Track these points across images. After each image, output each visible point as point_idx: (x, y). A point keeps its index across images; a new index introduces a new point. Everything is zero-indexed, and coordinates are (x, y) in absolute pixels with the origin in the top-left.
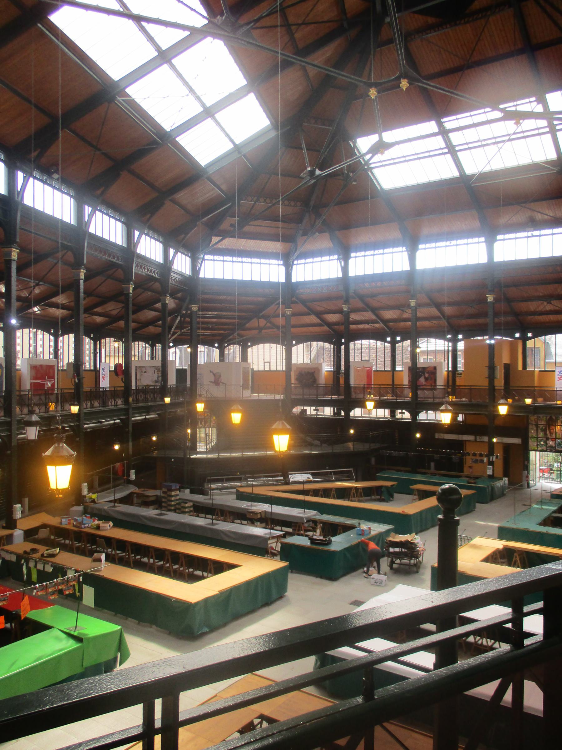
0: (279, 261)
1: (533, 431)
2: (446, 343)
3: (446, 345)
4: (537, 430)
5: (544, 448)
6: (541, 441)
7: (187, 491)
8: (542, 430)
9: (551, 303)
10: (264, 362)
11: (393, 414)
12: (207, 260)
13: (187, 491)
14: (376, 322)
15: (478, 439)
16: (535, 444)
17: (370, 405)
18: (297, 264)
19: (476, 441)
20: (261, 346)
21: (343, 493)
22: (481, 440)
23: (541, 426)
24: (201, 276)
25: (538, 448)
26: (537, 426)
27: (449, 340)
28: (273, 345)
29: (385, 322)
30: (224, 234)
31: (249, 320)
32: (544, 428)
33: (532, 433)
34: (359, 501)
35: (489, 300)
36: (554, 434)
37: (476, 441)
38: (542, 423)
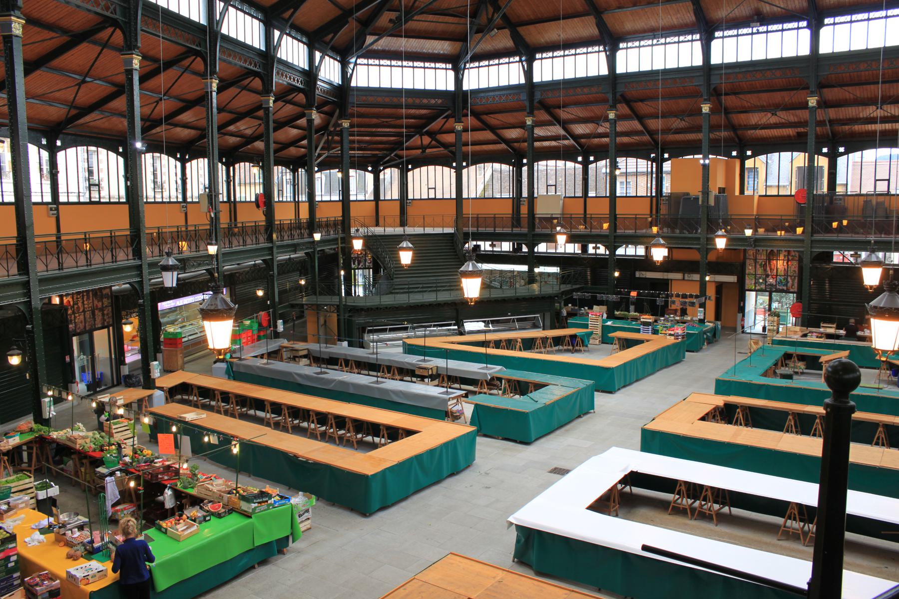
0: (447, 65)
1: (750, 268)
3: (649, 166)
4: (755, 266)
5: (763, 286)
6: (760, 278)
7: (345, 344)
8: (761, 265)
9: (776, 115)
10: (428, 189)
11: (584, 249)
12: (360, 64)
13: (345, 344)
14: (565, 138)
15: (686, 277)
17: (561, 239)
19: (684, 279)
20: (424, 169)
21: (529, 344)
22: (690, 279)
23: (761, 261)
24: (353, 84)
26: (755, 260)
27: (653, 160)
28: (439, 168)
29: (576, 137)
30: (380, 33)
31: (409, 137)
32: (763, 263)
33: (750, 269)
34: (548, 353)
36: (775, 270)
37: (684, 279)
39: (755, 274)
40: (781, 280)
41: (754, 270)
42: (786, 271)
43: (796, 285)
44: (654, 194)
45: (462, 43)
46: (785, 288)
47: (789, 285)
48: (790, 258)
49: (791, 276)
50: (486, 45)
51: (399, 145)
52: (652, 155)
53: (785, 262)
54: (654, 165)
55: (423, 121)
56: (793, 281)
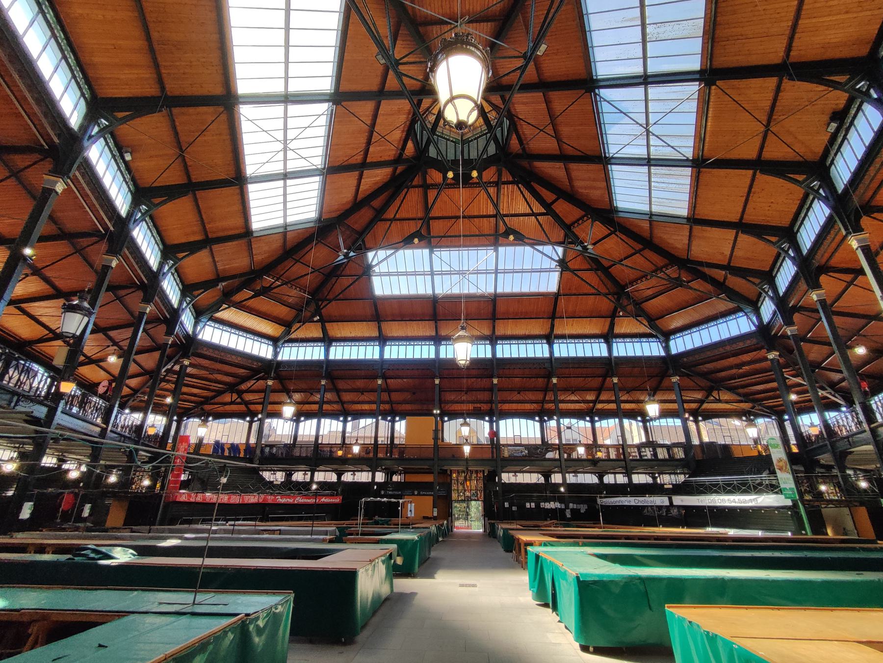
2: (387, 423)
5: (463, 498)
8: (461, 483)
12: (208, 325)
18: (284, 347)
24: (200, 337)
26: (457, 480)
27: (389, 421)
33: (454, 487)
35: (436, 383)
38: (461, 478)
39: (458, 490)
43: (483, 496)
44: (389, 443)
46: (476, 498)
47: (479, 496)
51: (207, 400)
52: (389, 418)
54: (390, 423)
55: (238, 380)
56: (481, 494)
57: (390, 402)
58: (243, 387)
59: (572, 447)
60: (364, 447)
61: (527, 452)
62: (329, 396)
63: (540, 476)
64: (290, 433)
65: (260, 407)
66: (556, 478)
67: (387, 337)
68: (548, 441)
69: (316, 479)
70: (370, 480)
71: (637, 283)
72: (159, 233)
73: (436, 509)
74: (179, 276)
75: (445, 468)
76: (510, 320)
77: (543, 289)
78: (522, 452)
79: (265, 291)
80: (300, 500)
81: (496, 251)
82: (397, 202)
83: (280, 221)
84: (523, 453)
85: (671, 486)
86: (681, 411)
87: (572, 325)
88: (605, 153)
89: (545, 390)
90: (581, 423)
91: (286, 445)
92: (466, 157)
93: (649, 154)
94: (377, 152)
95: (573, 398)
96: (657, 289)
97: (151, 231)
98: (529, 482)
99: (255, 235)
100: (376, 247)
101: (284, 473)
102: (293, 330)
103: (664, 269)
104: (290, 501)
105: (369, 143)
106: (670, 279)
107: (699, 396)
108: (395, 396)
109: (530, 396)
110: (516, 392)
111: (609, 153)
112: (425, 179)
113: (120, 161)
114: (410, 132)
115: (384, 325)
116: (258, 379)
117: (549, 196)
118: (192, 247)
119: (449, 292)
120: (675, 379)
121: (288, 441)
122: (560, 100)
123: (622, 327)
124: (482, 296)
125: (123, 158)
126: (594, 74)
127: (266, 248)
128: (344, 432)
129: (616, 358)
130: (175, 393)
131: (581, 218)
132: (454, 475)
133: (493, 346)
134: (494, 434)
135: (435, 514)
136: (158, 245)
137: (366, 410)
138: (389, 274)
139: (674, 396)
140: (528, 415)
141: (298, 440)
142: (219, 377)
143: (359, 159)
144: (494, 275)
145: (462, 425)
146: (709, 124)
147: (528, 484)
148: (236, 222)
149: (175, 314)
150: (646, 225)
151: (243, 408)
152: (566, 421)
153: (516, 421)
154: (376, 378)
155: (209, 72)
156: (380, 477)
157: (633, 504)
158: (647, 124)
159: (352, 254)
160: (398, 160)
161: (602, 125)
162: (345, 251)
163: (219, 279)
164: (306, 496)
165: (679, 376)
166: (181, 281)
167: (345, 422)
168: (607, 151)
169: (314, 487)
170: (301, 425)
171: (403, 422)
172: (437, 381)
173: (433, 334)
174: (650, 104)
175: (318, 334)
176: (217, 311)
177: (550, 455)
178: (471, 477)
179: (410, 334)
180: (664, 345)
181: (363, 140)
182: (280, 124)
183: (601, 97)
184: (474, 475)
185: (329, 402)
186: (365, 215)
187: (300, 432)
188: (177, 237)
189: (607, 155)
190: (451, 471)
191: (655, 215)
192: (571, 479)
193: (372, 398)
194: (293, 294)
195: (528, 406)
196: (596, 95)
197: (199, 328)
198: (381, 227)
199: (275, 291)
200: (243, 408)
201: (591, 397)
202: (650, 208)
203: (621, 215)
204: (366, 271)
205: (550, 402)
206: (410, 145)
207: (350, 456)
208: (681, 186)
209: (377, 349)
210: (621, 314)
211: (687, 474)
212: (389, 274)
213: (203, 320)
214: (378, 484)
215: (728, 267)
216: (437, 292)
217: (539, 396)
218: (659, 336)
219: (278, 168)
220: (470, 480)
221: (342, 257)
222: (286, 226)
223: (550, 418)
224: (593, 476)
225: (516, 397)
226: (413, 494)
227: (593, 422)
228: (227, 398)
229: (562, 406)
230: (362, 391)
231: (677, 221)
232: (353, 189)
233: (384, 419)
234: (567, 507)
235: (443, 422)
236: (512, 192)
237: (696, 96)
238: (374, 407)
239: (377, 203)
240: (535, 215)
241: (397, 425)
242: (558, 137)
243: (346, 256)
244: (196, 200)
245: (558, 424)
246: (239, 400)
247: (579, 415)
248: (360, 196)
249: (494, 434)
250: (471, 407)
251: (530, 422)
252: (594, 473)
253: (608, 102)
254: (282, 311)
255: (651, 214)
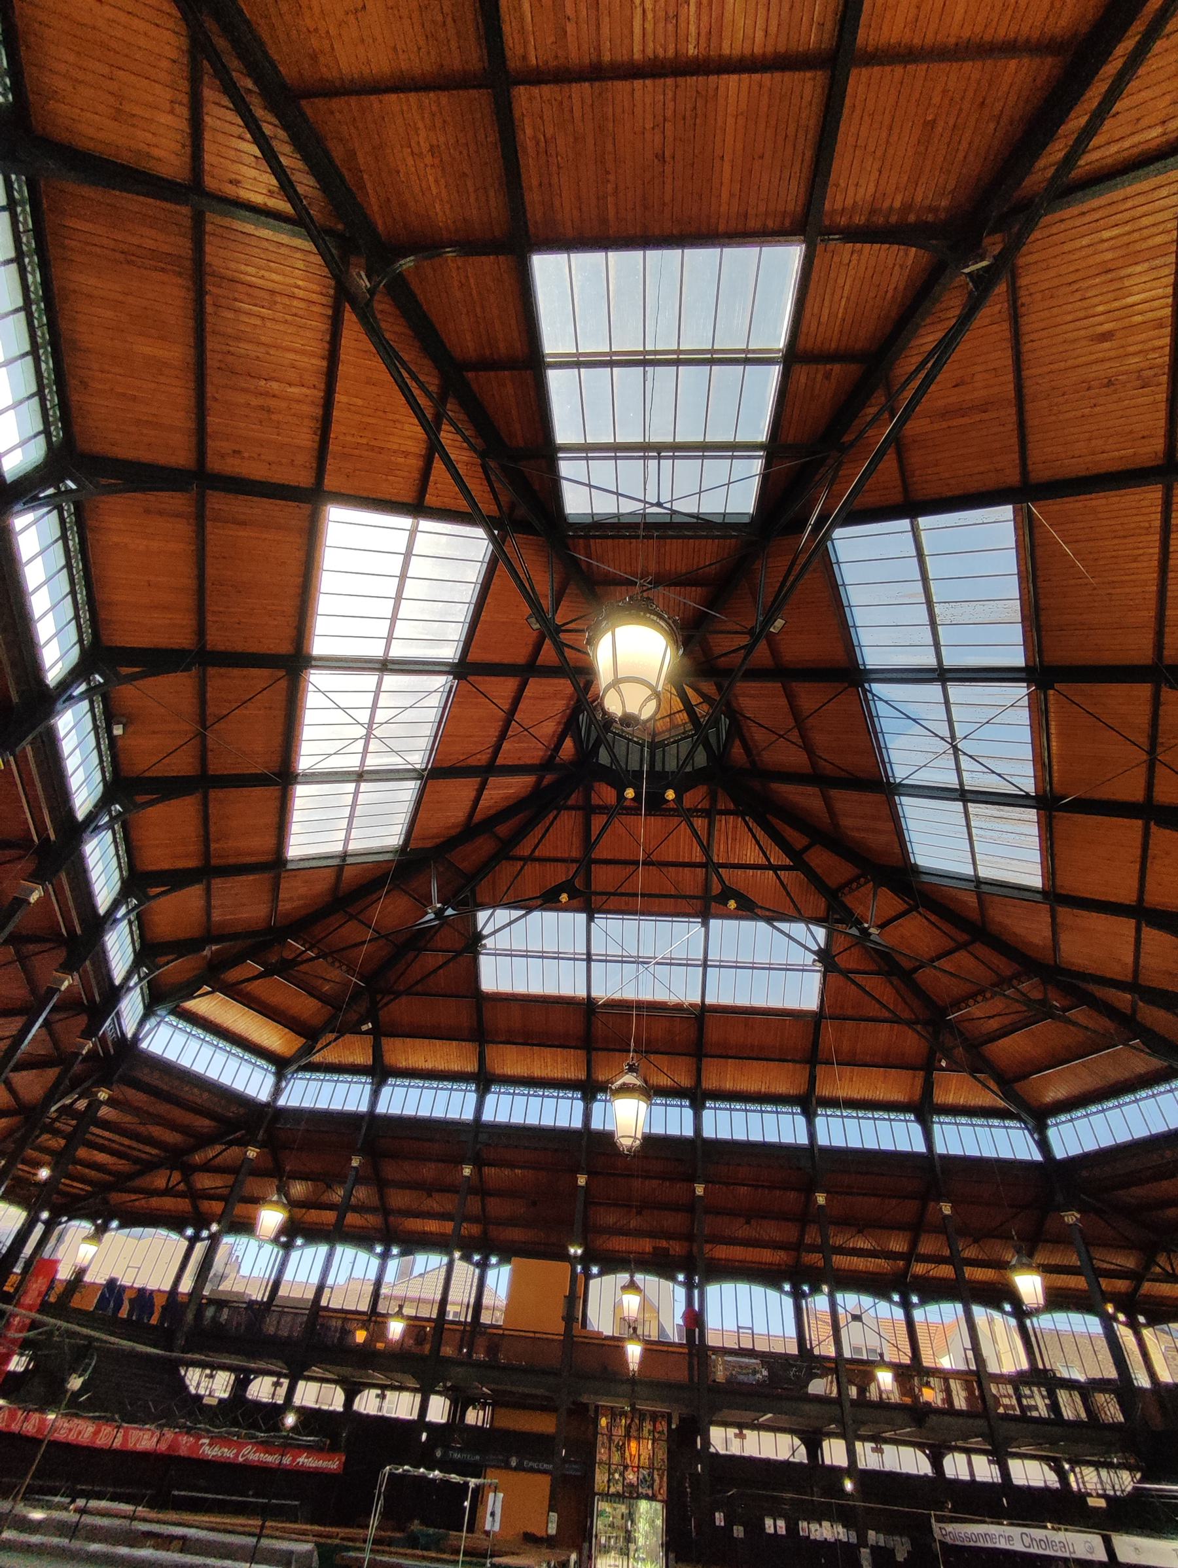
2: (471, 1268)
5: (620, 1488)
6: (616, 1471)
16: (606, 1479)
18: (296, 1078)
24: (144, 1045)
25: (609, 1487)
27: (477, 1265)
33: (602, 1454)
39: (610, 1465)
40: (644, 1478)
41: (607, 1456)
42: (651, 1459)
43: (665, 1485)
44: (469, 1320)
45: (303, 1040)
47: (656, 1486)
48: (657, 1435)
49: (658, 1470)
50: (329, 1055)
51: (120, 1182)
53: (650, 1442)
57: (482, 1219)
58: (198, 1158)
59: (861, 1371)
60: (415, 1326)
61: (765, 1373)
62: (362, 1194)
63: (797, 1442)
64: (267, 1276)
65: (217, 1207)
66: (834, 1452)
67: (494, 1075)
68: (812, 1348)
69: (297, 1401)
70: (415, 1416)
71: (968, 1006)
72: (129, 851)
73: (554, 1516)
74: (140, 927)
75: (585, 1399)
76: (730, 1060)
77: (792, 1003)
78: (755, 1372)
79: (285, 968)
80: (251, 1454)
81: (705, 924)
82: (539, 831)
83: (338, 848)
84: (758, 1376)
85: (1102, 1503)
86: (1098, 1297)
87: (851, 1080)
88: (887, 777)
89: (805, 1216)
90: (883, 1307)
91: (252, 1303)
92: (658, 768)
93: (961, 783)
94: (511, 752)
95: (862, 1243)
96: (1007, 1020)
97: (116, 847)
98: (772, 1456)
99: (290, 866)
100: (495, 904)
101: (233, 1377)
102: (319, 1046)
103: (1015, 982)
104: (228, 1453)
105: (503, 736)
106: (1028, 1001)
107: (1128, 1262)
108: (496, 1206)
109: (771, 1230)
110: (742, 1220)
111: (893, 776)
112: (588, 798)
113: (102, 732)
114: (570, 725)
115: (492, 1051)
116: (230, 1144)
117: (798, 840)
118: (176, 879)
119: (617, 996)
120: (1071, 1217)
121: (258, 1294)
122: (809, 696)
123: (947, 1091)
124: (678, 1008)
125: (109, 730)
126: (860, 662)
127: (303, 890)
128: (378, 1283)
129: (943, 1157)
130: (59, 1160)
131: (856, 879)
132: (603, 1422)
133: (698, 1109)
134: (695, 1320)
135: (552, 1530)
136: (121, 871)
137: (431, 1233)
138: (511, 954)
139: (1075, 1257)
140: (769, 1277)
141: (280, 1293)
142: (157, 1131)
143: (483, 759)
144: (701, 969)
145: (625, 1288)
146: (1054, 744)
147: (767, 1462)
148: (261, 844)
149: (113, 994)
150: (972, 900)
151: (184, 1205)
152: (849, 1301)
153: (743, 1288)
154: (462, 1161)
155: (276, 623)
156: (438, 1410)
157: (1018, 1546)
158: (953, 737)
159: (450, 912)
160: (548, 764)
161: (880, 735)
162: (439, 905)
163: (209, 935)
164: (266, 1446)
165: (1079, 1211)
166: (141, 936)
167: (385, 1256)
168: (890, 774)
169: (290, 1420)
170: (295, 1255)
171: (506, 1270)
172: (582, 1180)
173: (582, 1076)
174: (953, 709)
175: (363, 1057)
176: (191, 996)
177: (819, 1386)
178: (640, 1429)
179: (538, 1072)
180: (1036, 1136)
181: (494, 732)
182: (368, 700)
183: (874, 695)
184: (648, 1426)
185: (360, 1209)
186: (484, 846)
187: (288, 1276)
188: (158, 859)
189: (892, 780)
190: (597, 1407)
191: (986, 883)
192: (869, 1457)
193: (449, 1207)
194: (333, 976)
195: (768, 1256)
196: (865, 691)
197: (147, 1027)
198: (507, 870)
199: (303, 967)
200: (184, 1205)
201: (898, 1244)
202: (975, 869)
203: (926, 878)
204: (473, 942)
205: (813, 1248)
206: (568, 743)
207: (380, 1346)
208: (1023, 837)
209: (472, 1097)
210: (944, 1064)
211: (1138, 1469)
212: (511, 954)
213: (159, 1012)
214: (432, 1428)
215: (1133, 986)
216: (595, 994)
217: (789, 1233)
218: (1024, 1116)
219: (351, 762)
220: (638, 1439)
221: (432, 916)
222: (344, 855)
223: (815, 1290)
224: (919, 1453)
225: (742, 1230)
226: (507, 1466)
227: (906, 1306)
228: (159, 1181)
229: (840, 1261)
230: (428, 1188)
231: (1027, 895)
232: (467, 804)
233: (467, 1258)
234: (863, 1541)
235: (588, 1276)
236: (735, 827)
237: (1025, 702)
238: (448, 1227)
239: (503, 830)
240: (775, 868)
241: (491, 1274)
242: (808, 748)
243: (439, 914)
244: (205, 804)
245: (833, 1305)
246: (182, 1186)
247: (876, 1286)
248: (478, 817)
249: (695, 1320)
250: (647, 1245)
251: (773, 1294)
252: (920, 1446)
253: (886, 702)
254: (306, 1006)
255: (978, 882)
